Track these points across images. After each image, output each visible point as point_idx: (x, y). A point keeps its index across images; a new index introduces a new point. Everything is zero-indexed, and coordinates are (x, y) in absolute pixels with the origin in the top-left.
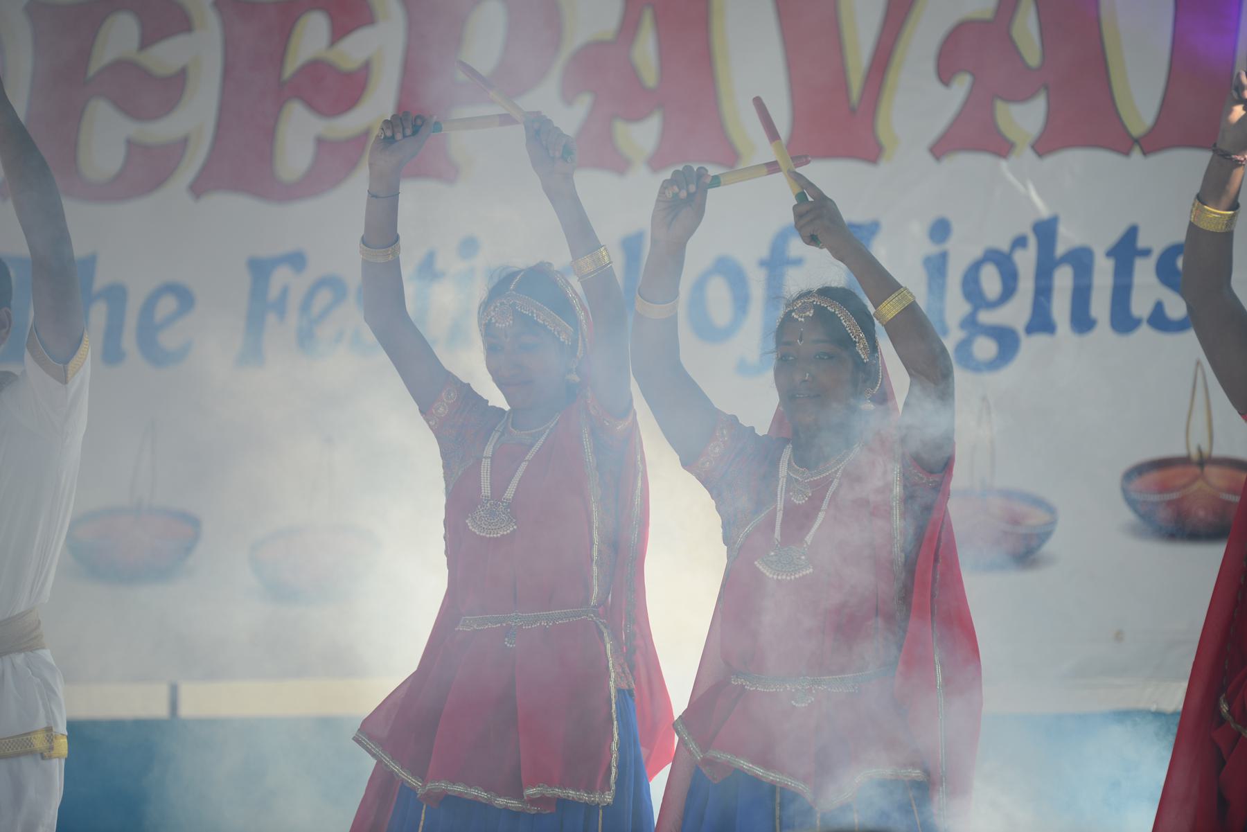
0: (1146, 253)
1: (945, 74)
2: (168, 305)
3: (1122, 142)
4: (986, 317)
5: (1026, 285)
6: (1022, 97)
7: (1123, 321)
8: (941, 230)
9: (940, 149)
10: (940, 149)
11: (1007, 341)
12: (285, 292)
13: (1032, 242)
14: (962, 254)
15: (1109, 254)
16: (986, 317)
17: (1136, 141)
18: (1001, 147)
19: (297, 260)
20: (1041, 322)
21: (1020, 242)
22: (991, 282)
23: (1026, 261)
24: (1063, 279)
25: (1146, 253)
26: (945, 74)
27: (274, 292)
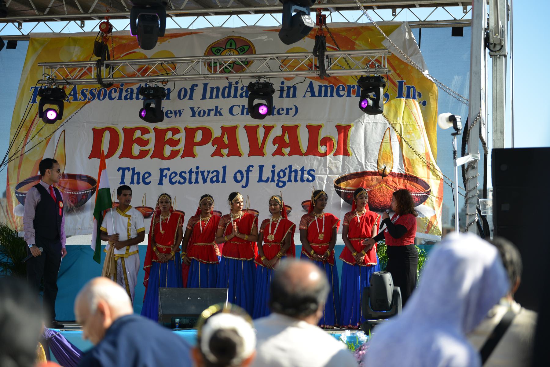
0: (306, 170)
1: (274, 144)
2: (147, 175)
3: (301, 154)
4: (281, 179)
5: (287, 175)
6: (286, 147)
7: (302, 180)
8: (274, 167)
9: (273, 155)
10: (273, 155)
11: (284, 183)
12: (166, 174)
13: (288, 168)
14: (277, 170)
15: (300, 171)
16: (281, 179)
17: (303, 154)
18: (283, 155)
19: (168, 169)
20: (290, 180)
21: (286, 169)
22: (282, 174)
23: (287, 171)
24: (293, 174)
25: (306, 170)
26: (274, 144)
27: (164, 174)
